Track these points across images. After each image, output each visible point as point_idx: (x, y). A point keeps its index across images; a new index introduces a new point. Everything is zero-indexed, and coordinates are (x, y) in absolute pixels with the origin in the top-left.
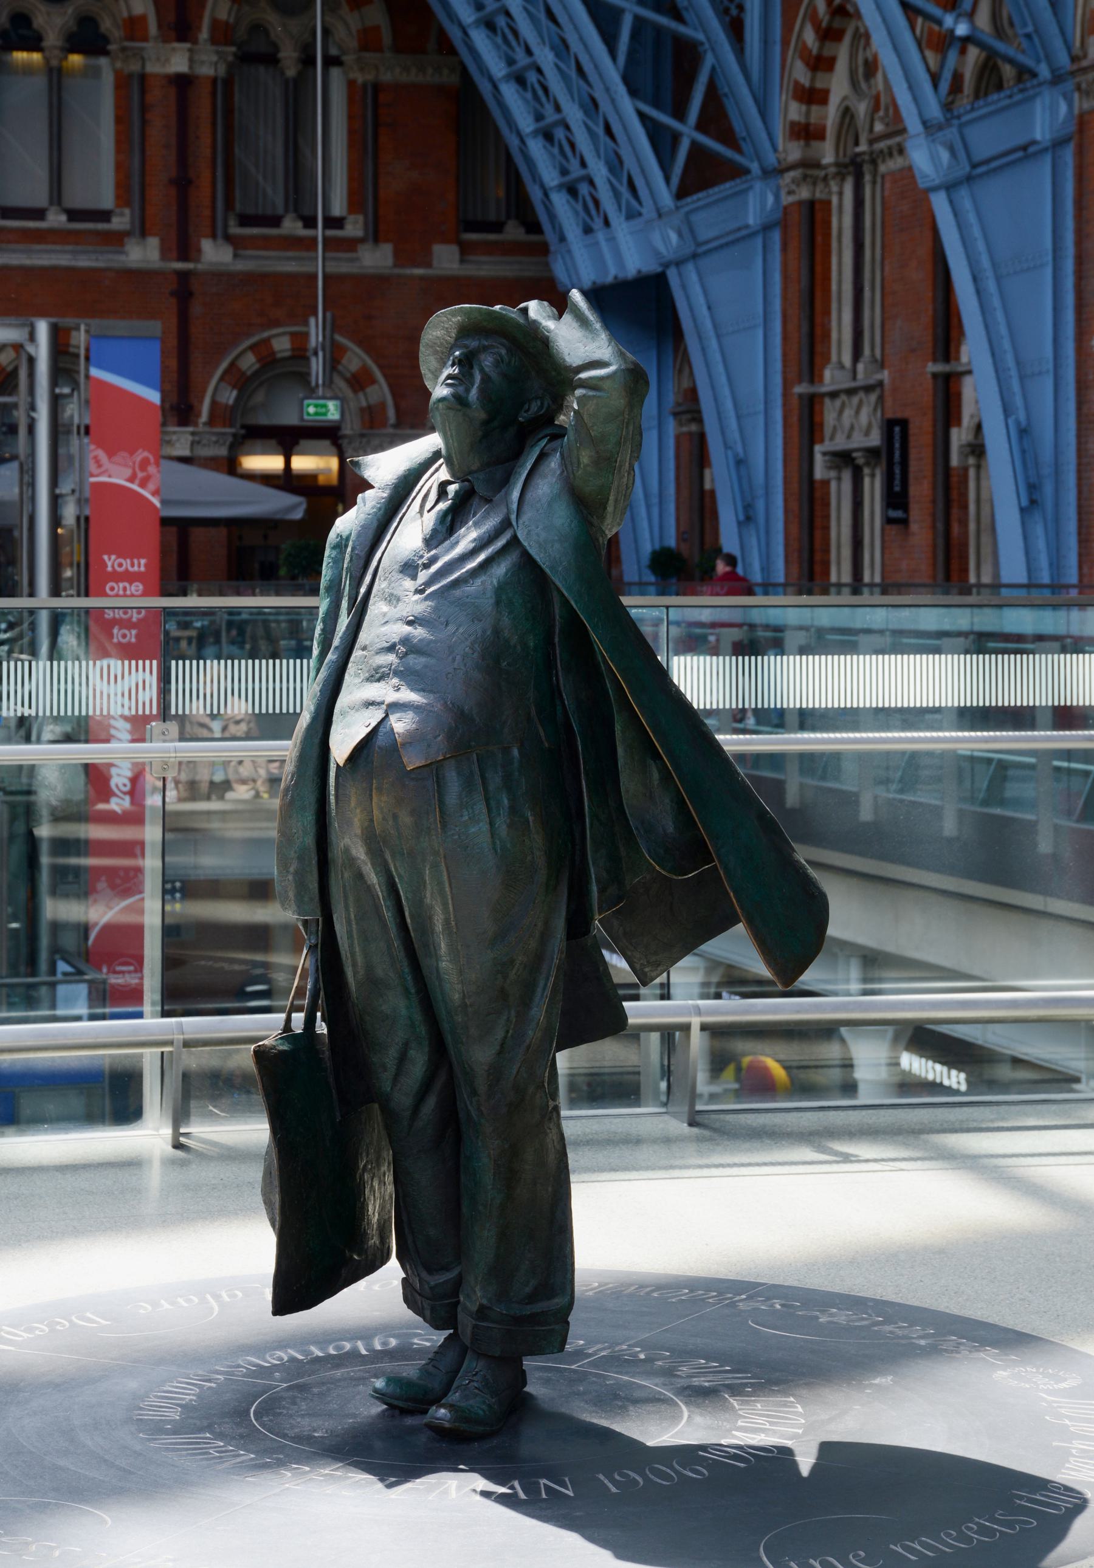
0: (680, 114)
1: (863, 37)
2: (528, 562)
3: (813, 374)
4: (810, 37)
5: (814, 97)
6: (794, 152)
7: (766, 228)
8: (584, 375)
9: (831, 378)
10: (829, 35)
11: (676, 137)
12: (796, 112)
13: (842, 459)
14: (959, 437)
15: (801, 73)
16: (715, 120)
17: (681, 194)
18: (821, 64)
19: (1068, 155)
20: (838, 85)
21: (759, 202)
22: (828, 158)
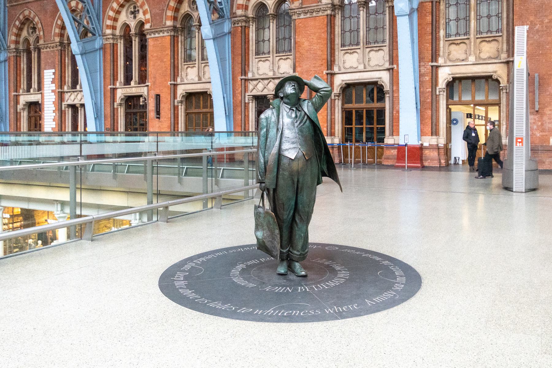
2: (312, 122)
8: (324, 89)
19: (7, 64)
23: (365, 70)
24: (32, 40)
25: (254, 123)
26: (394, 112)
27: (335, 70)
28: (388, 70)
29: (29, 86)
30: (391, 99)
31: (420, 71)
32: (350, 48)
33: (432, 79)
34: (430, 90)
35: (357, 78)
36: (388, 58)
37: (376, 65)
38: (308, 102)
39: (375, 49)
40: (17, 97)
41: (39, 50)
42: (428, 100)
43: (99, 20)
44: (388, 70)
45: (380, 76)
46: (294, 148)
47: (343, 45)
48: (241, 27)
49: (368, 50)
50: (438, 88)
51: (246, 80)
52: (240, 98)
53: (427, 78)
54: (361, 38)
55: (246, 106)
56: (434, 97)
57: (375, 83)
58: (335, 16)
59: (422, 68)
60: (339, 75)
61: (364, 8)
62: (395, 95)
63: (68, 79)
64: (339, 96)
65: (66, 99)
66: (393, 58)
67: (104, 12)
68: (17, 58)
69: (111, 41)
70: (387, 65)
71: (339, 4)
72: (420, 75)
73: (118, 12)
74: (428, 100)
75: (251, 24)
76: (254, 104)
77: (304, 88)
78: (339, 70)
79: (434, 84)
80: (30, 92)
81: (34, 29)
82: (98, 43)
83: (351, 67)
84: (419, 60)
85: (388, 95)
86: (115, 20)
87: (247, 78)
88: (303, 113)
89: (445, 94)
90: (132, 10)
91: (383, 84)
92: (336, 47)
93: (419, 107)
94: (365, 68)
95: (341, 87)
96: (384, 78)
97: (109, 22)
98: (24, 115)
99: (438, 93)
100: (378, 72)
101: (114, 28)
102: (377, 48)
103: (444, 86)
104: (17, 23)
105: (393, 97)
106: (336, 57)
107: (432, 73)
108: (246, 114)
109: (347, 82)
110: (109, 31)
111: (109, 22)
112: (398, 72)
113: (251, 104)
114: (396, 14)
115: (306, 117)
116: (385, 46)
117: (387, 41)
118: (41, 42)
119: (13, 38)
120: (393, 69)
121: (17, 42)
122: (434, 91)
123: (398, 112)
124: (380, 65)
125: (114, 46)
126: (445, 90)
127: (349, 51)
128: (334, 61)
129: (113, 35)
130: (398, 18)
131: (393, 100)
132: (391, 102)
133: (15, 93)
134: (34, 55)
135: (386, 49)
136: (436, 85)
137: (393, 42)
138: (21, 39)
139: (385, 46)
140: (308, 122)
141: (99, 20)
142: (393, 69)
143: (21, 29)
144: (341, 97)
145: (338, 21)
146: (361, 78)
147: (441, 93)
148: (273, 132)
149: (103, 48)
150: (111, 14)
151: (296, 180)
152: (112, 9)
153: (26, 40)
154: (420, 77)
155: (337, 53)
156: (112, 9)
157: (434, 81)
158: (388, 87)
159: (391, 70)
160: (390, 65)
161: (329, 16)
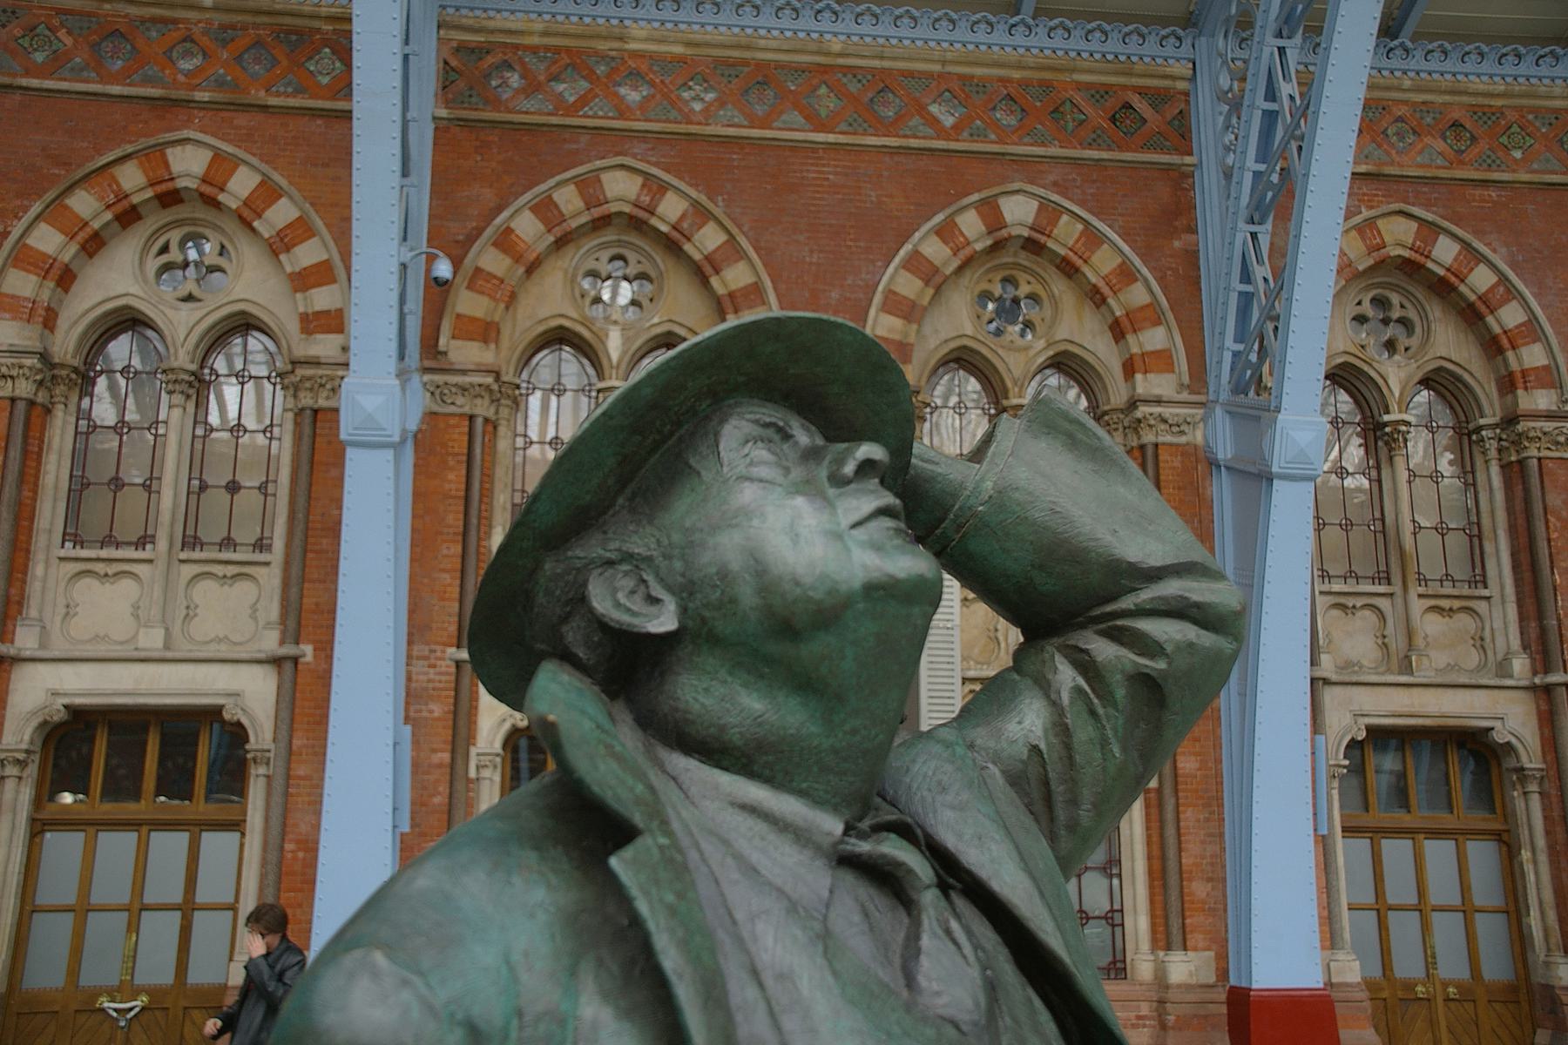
23: (169, 655)
26: (289, 846)
27: (18, 642)
28: (276, 661)
30: (278, 784)
31: (409, 679)
32: (104, 553)
33: (455, 713)
34: (446, 757)
35: (127, 685)
36: (274, 611)
37: (219, 640)
39: (219, 570)
42: (437, 800)
44: (276, 661)
45: (234, 686)
47: (73, 536)
49: (188, 571)
50: (473, 751)
53: (437, 709)
54: (165, 517)
56: (460, 786)
57: (212, 714)
58: (48, 411)
59: (419, 666)
60: (41, 667)
61: (188, 397)
62: (301, 770)
64: (22, 764)
66: (309, 612)
70: (270, 643)
71: (75, 363)
72: (408, 694)
74: (437, 800)
78: (42, 646)
79: (463, 731)
83: (97, 638)
84: (410, 634)
85: (262, 770)
89: (497, 778)
91: (245, 721)
92: (40, 542)
93: (406, 828)
94: (167, 647)
95: (45, 723)
96: (253, 695)
99: (472, 774)
100: (227, 669)
102: (231, 570)
103: (497, 746)
105: (288, 777)
106: (34, 588)
107: (457, 690)
109: (78, 701)
112: (324, 678)
114: (343, 436)
116: (267, 564)
117: (279, 544)
120: (295, 660)
122: (459, 762)
123: (310, 847)
124: (236, 638)
126: (498, 760)
127: (100, 568)
128: (20, 604)
130: (351, 453)
131: (287, 794)
132: (277, 799)
135: (271, 578)
136: (471, 738)
137: (305, 551)
139: (267, 564)
142: (295, 660)
144: (32, 770)
145: (60, 433)
146: (143, 686)
147: (486, 773)
154: (407, 703)
155: (38, 569)
157: (462, 723)
158: (269, 735)
159: (288, 666)
160: (282, 643)
161: (21, 406)
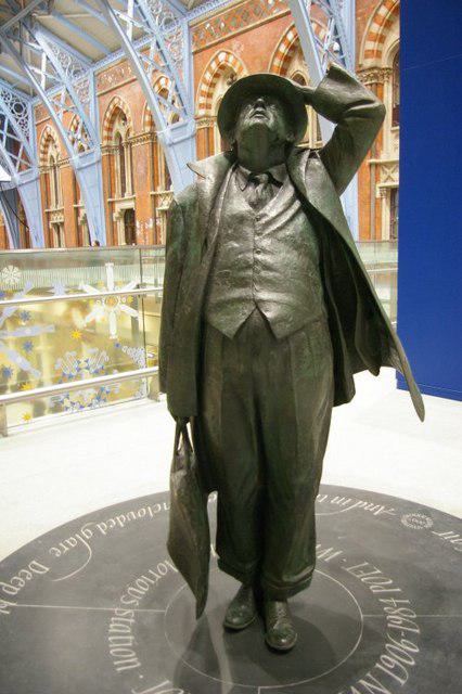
0: (17, 155)
1: (54, 141)
3: (48, 208)
4: (43, 141)
5: (45, 153)
6: (41, 164)
7: (37, 179)
9: (52, 209)
10: (47, 140)
11: (22, 157)
12: (41, 155)
13: (56, 225)
14: (80, 219)
15: (42, 148)
16: (25, 156)
17: (20, 169)
18: (46, 146)
19: (100, 166)
20: (51, 151)
21: (36, 172)
22: (48, 165)
24: (123, 134)
25: (388, 223)
29: (124, 190)
38: (312, 155)
40: (112, 203)
41: (130, 144)
43: (190, 99)
46: (241, 300)
48: (371, 85)
51: (377, 165)
52: (368, 192)
55: (378, 203)
63: (162, 181)
65: (160, 203)
67: (196, 87)
68: (110, 157)
69: (205, 125)
73: (212, 85)
75: (386, 79)
76: (389, 200)
77: (304, 113)
80: (123, 196)
81: (125, 119)
82: (192, 127)
86: (210, 96)
87: (377, 161)
88: (289, 192)
90: (230, 80)
97: (202, 100)
98: (121, 226)
101: (208, 107)
104: (108, 115)
108: (378, 215)
110: (202, 112)
111: (202, 100)
113: (384, 200)
115: (297, 204)
118: (131, 135)
119: (105, 133)
121: (109, 138)
125: (209, 130)
129: (205, 116)
133: (110, 200)
134: (127, 152)
138: (114, 134)
140: (301, 219)
141: (190, 99)
143: (112, 122)
148: (195, 248)
149: (196, 136)
150: (204, 88)
151: (250, 401)
152: (205, 81)
153: (119, 137)
156: (205, 81)
